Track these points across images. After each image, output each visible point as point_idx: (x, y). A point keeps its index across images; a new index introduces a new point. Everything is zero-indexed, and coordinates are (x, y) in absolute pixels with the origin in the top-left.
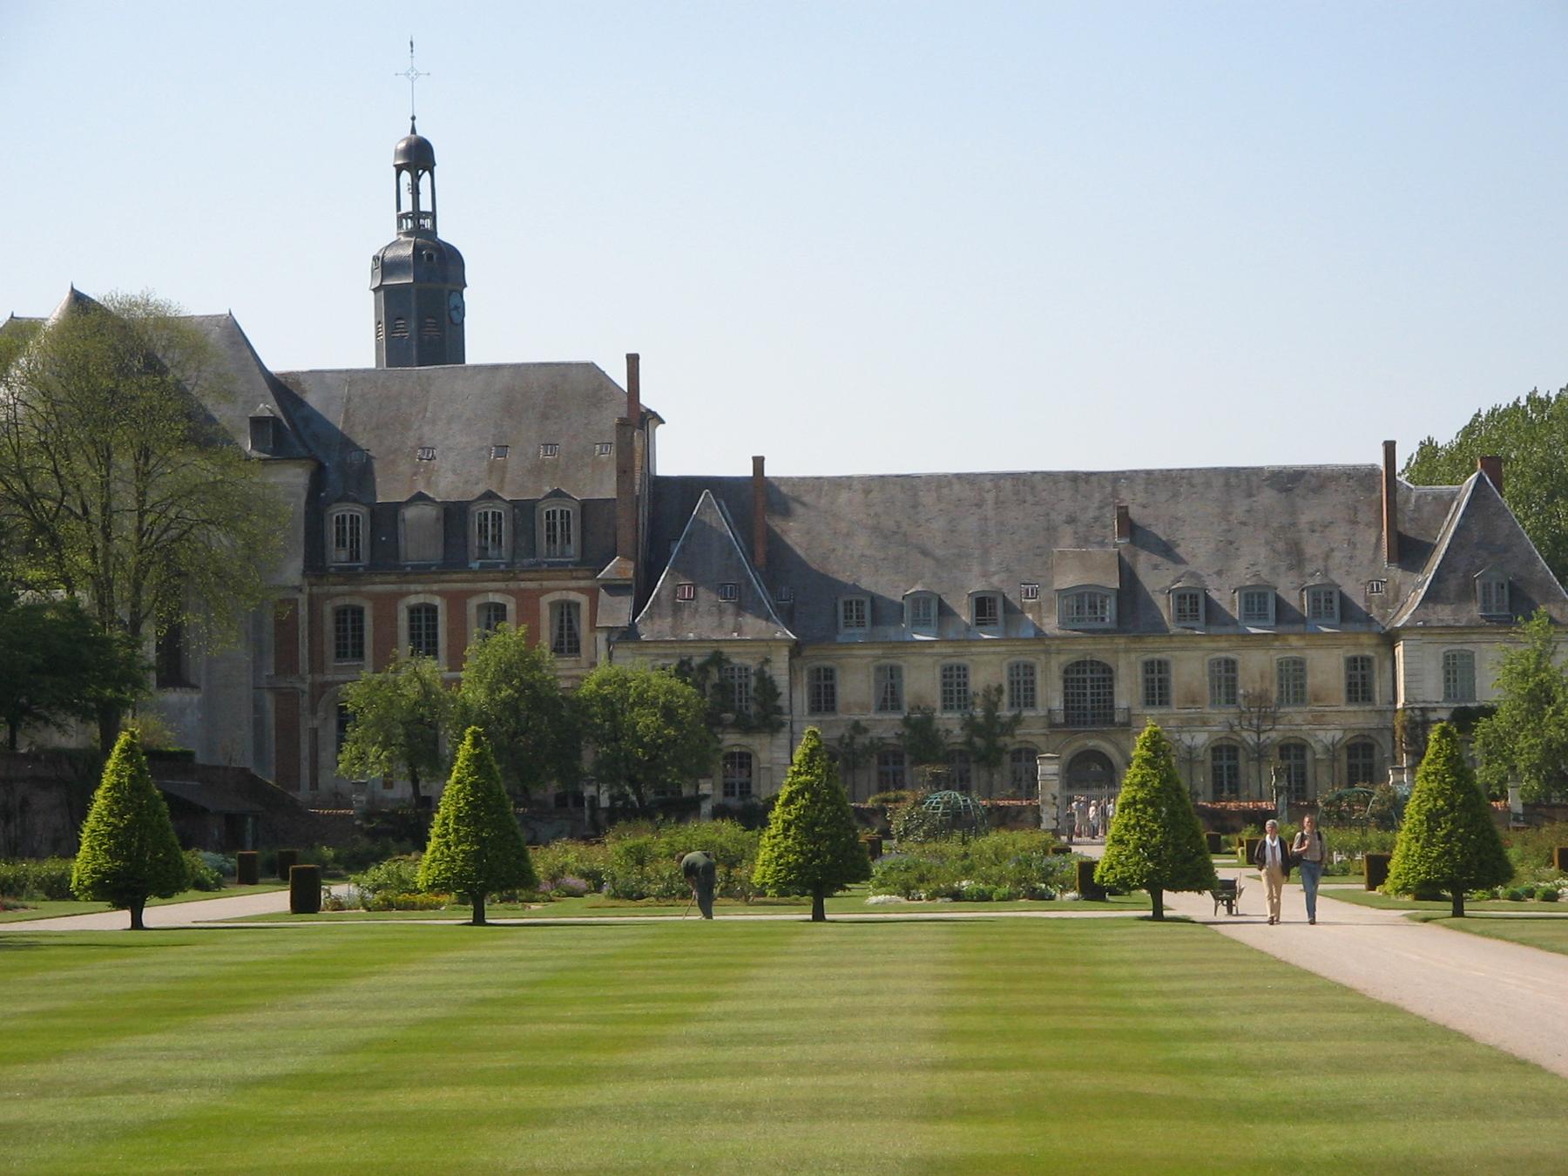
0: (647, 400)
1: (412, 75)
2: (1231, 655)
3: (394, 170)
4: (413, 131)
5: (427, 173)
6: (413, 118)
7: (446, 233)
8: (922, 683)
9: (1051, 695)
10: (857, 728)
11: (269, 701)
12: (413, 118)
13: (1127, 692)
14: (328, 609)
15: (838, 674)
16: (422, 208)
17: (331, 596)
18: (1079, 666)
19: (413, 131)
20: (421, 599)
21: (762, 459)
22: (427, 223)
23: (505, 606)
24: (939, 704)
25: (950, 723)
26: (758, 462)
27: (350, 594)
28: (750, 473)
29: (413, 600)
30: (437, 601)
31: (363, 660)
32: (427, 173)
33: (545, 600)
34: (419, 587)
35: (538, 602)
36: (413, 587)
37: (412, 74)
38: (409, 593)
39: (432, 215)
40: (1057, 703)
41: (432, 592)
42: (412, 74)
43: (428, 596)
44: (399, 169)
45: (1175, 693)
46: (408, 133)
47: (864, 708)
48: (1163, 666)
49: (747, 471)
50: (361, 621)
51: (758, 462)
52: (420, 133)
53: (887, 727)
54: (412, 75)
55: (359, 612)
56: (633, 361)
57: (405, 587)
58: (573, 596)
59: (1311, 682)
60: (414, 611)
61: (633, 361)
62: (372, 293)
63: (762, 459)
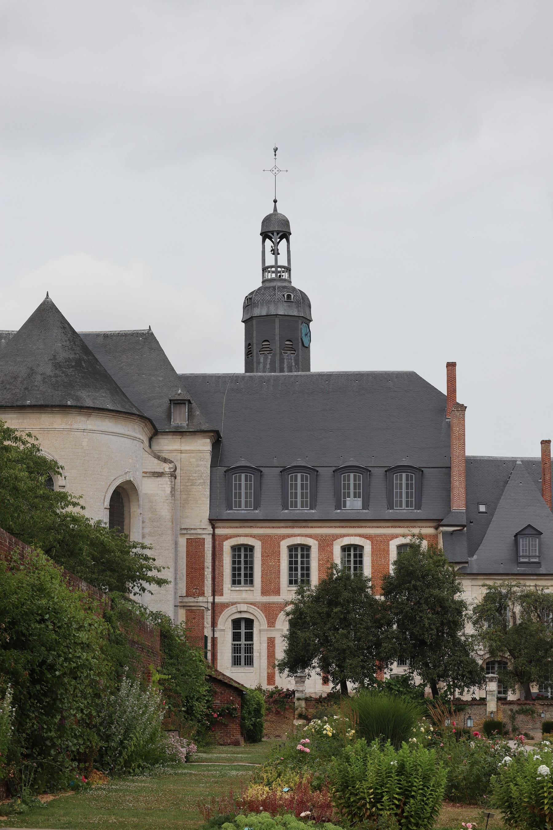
0: (460, 399)
1: (275, 171)
3: (261, 238)
4: (275, 209)
5: (284, 240)
6: (275, 201)
7: (297, 283)
12: (275, 201)
14: (227, 546)
16: (279, 264)
17: (227, 537)
19: (275, 209)
20: (298, 540)
21: (549, 442)
22: (285, 276)
23: (363, 547)
27: (246, 536)
28: (539, 455)
31: (253, 586)
32: (284, 240)
35: (389, 544)
37: (275, 171)
38: (289, 536)
39: (288, 269)
41: (307, 536)
42: (275, 171)
43: (303, 538)
44: (265, 235)
46: (272, 212)
49: (536, 453)
50: (252, 556)
54: (275, 171)
55: (250, 549)
56: (451, 366)
60: (292, 549)
61: (451, 366)
62: (243, 324)
63: (549, 442)
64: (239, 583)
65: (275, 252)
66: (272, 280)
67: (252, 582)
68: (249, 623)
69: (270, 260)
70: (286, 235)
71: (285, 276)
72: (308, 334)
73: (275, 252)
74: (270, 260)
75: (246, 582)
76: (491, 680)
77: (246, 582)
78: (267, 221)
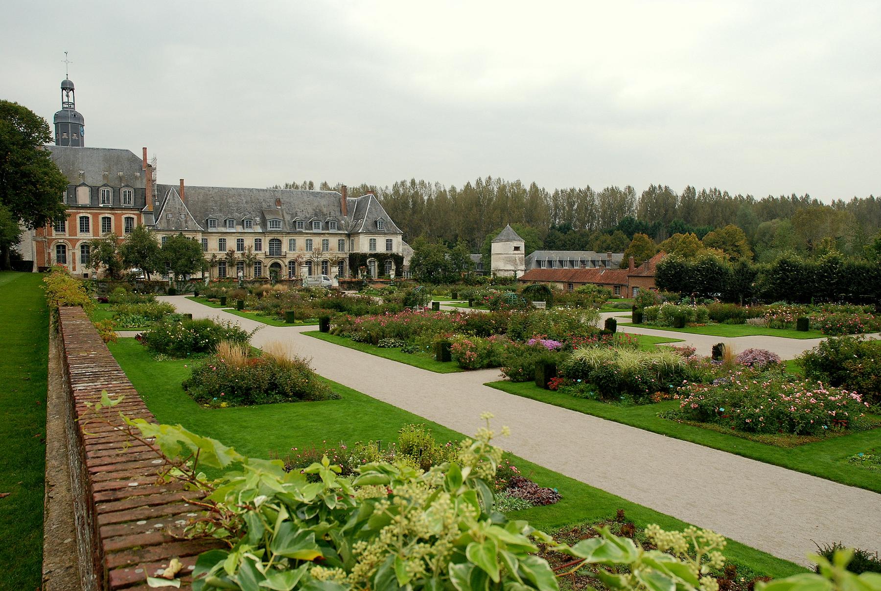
2: (311, 238)
7: (78, 109)
8: (231, 243)
9: (266, 247)
10: (214, 256)
11: (34, 243)
13: (285, 248)
15: (208, 240)
18: (272, 240)
20: (84, 215)
24: (236, 250)
25: (238, 255)
26: (182, 181)
29: (81, 215)
30: (89, 215)
33: (101, 217)
34: (83, 211)
36: (81, 211)
38: (80, 213)
39: (74, 104)
40: (268, 250)
44: (63, 89)
45: (297, 248)
47: (216, 250)
48: (294, 240)
51: (182, 181)
52: (69, 79)
53: (221, 255)
54: (67, 62)
56: (145, 149)
57: (79, 211)
58: (132, 216)
59: (330, 245)
61: (145, 149)
64: (59, 231)
65: (68, 96)
66: (67, 108)
67: (64, 231)
68: (64, 247)
69: (65, 100)
70: (73, 90)
71: (72, 106)
72: (83, 131)
73: (68, 96)
74: (65, 100)
75: (62, 231)
76: (171, 273)
77: (62, 231)
78: (63, 83)
